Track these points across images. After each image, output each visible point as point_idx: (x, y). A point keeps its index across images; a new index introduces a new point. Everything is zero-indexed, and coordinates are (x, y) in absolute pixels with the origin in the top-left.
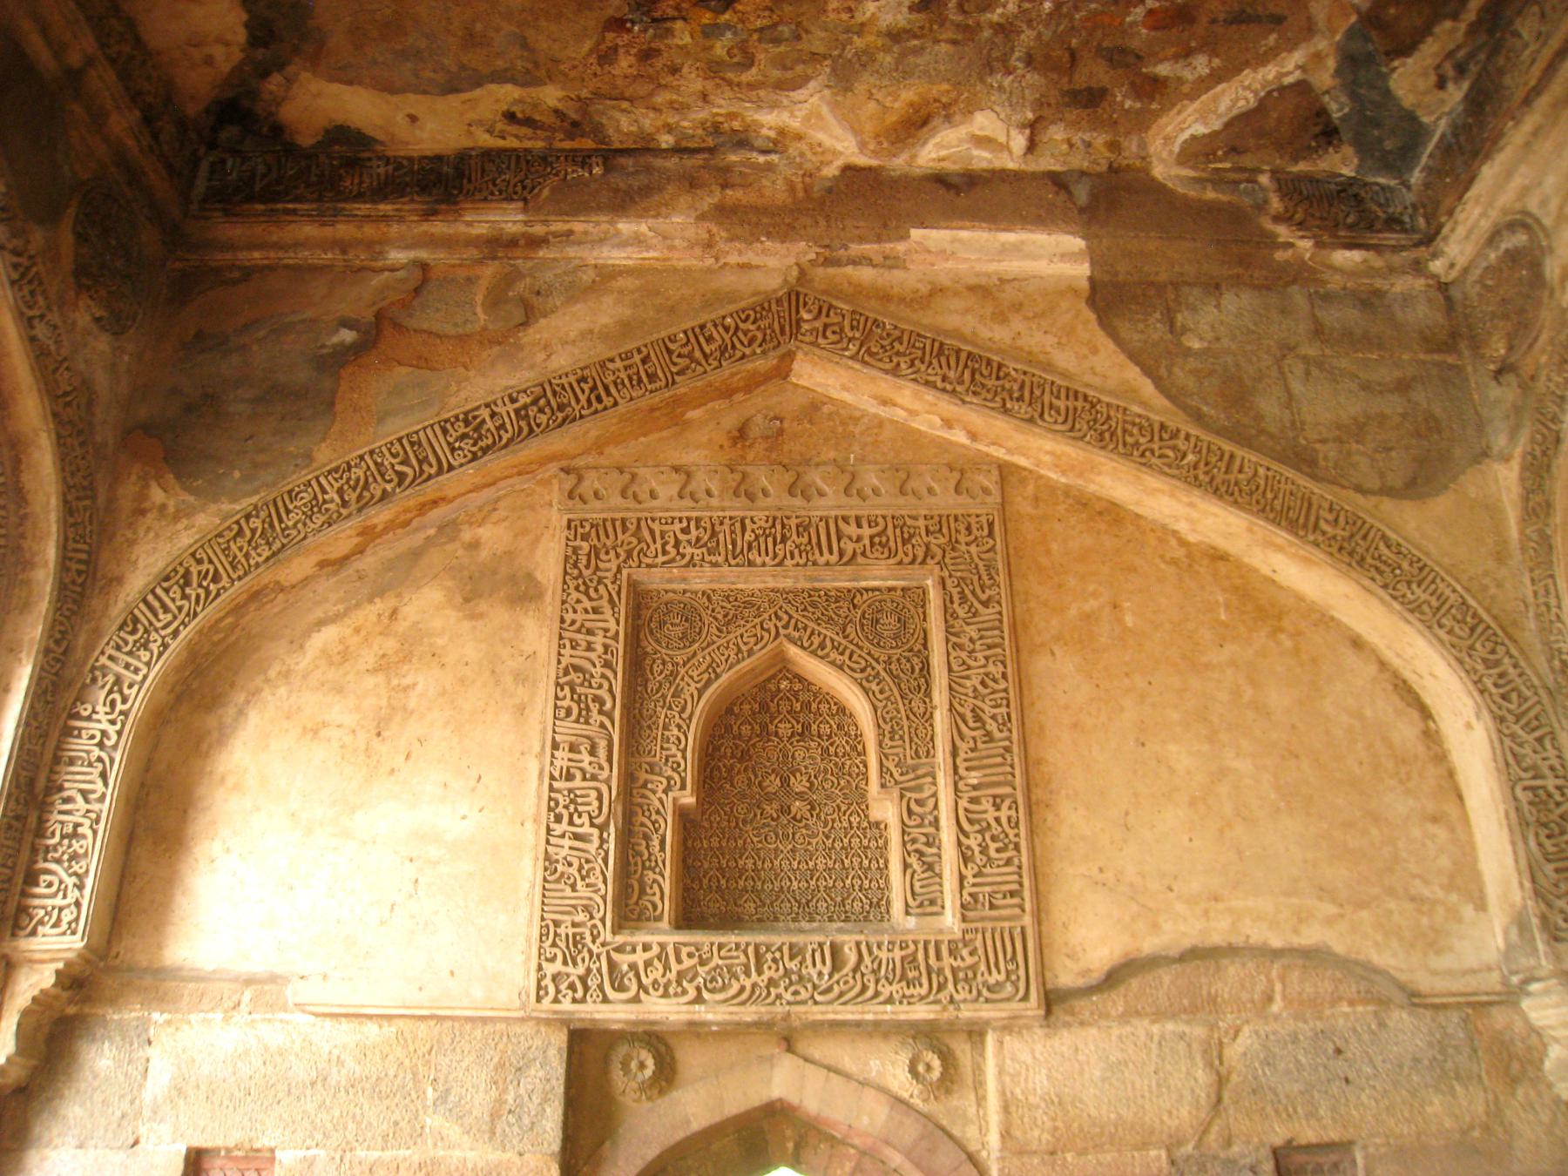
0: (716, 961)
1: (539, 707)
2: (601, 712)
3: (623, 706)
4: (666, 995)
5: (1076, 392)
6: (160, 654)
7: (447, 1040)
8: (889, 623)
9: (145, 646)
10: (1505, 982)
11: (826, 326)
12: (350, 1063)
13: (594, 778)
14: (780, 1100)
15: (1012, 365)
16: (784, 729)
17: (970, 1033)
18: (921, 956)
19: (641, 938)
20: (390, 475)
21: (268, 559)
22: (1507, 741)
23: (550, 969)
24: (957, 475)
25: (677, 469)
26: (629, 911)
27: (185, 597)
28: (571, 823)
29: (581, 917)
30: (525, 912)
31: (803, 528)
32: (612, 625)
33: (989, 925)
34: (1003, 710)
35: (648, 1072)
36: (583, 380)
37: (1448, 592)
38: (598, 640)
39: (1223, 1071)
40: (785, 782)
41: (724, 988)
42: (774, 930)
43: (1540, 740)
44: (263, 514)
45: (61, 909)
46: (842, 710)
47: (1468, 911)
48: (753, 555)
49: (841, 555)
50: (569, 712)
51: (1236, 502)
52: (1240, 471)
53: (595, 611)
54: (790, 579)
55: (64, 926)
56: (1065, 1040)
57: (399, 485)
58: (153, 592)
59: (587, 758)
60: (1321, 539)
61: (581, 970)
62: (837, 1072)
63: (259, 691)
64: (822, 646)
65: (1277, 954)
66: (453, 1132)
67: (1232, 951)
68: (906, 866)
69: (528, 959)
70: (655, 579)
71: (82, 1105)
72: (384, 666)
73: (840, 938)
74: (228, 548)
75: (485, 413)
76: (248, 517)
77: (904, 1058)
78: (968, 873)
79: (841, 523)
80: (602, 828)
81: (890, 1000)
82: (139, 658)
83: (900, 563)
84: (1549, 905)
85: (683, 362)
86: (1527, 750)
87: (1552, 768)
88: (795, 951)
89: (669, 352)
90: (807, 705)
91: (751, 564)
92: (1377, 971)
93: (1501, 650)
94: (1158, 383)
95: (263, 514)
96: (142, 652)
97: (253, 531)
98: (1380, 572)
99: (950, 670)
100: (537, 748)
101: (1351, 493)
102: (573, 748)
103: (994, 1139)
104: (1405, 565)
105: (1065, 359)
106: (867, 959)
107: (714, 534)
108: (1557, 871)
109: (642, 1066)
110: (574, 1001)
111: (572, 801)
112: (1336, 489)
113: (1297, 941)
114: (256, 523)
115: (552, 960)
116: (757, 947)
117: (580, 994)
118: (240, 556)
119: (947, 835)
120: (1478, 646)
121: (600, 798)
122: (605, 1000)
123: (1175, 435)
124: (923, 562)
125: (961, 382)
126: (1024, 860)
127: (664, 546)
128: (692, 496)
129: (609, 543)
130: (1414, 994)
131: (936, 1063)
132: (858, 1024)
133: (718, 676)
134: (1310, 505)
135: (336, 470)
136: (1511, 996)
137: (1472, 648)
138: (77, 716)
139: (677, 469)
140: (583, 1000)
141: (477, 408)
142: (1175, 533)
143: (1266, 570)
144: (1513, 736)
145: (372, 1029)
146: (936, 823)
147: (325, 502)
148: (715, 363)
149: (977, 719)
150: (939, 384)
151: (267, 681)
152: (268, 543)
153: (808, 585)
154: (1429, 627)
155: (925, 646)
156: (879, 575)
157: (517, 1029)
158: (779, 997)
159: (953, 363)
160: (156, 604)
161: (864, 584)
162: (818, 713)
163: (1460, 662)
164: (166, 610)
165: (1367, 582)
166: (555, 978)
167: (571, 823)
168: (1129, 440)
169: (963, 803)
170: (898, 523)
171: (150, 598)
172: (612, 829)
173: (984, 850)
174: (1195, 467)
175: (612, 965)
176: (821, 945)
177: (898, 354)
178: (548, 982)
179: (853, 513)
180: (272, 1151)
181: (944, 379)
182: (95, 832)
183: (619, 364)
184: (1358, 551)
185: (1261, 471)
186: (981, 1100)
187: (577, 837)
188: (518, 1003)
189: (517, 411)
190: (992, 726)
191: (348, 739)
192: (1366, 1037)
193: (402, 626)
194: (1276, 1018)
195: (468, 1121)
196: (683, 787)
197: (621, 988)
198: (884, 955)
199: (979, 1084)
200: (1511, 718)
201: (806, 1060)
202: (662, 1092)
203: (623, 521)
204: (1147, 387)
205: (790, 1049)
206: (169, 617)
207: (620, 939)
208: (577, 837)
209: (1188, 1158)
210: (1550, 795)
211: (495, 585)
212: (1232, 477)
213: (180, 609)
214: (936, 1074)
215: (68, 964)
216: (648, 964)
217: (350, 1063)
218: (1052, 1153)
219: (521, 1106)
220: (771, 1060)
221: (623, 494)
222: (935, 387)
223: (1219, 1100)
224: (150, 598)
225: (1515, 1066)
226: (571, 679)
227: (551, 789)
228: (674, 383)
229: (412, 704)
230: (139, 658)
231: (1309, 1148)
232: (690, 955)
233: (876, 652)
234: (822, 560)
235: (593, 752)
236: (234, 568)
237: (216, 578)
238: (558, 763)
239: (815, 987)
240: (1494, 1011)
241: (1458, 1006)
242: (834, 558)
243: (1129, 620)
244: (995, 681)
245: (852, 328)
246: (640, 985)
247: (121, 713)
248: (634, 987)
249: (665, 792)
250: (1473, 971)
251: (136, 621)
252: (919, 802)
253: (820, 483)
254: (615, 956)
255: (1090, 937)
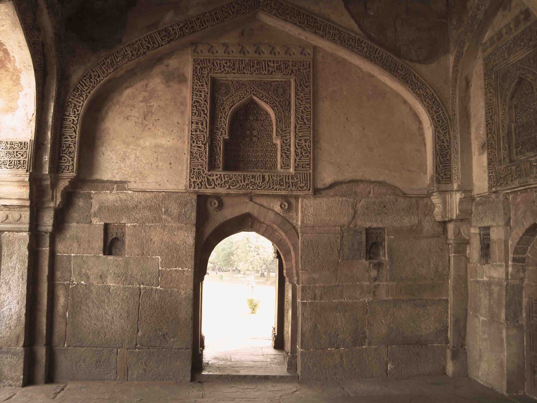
0: (234, 179)
1: (187, 112)
2: (204, 114)
3: (210, 113)
4: (221, 187)
5: (336, 28)
6: (86, 98)
7: (167, 197)
8: (281, 91)
9: (81, 96)
10: (428, 192)
11: (267, 4)
12: (143, 203)
13: (203, 131)
14: (249, 213)
15: (318, 18)
16: (251, 118)
17: (295, 198)
18: (284, 179)
19: (215, 173)
20: (145, 47)
21: (113, 71)
22: (437, 133)
23: (192, 180)
24: (301, 49)
25: (224, 44)
26: (212, 166)
27: (91, 82)
28: (197, 143)
29: (200, 167)
30: (185, 166)
31: (258, 63)
32: (206, 90)
33: (302, 172)
34: (309, 116)
35: (216, 205)
36: (198, 19)
37: (429, 92)
38: (203, 94)
39: (356, 210)
40: (251, 132)
41: (236, 185)
42: (247, 171)
43: (445, 133)
44: (110, 58)
45: (69, 166)
46: (267, 113)
47: (422, 174)
48: (245, 71)
49: (269, 71)
50: (195, 113)
51: (376, 63)
52: (378, 54)
53: (202, 85)
54: (255, 77)
55: (70, 170)
56: (318, 201)
57: (148, 49)
58: (81, 80)
59: (201, 126)
60: (397, 74)
61: (200, 181)
62: (262, 206)
63: (111, 106)
64: (263, 97)
65: (373, 182)
66: (169, 219)
67: (362, 181)
68: (282, 156)
69: (187, 177)
70: (218, 76)
71: (77, 213)
72: (145, 100)
73: (264, 174)
74: (101, 68)
75: (171, 29)
76: (106, 59)
77: (279, 203)
78: (297, 159)
79: (269, 63)
80: (205, 145)
81: (276, 190)
82: (80, 99)
83: (284, 74)
84: (439, 175)
85: (226, 14)
86: (441, 136)
87: (447, 141)
88: (253, 177)
89: (223, 11)
90: (257, 112)
91: (244, 73)
92: (396, 187)
93: (440, 109)
94: (359, 26)
95: (110, 58)
96: (81, 98)
97: (108, 63)
98: (412, 86)
99: (296, 105)
100: (187, 123)
101: (407, 62)
102: (197, 123)
103: (299, 223)
104: (419, 84)
105: (333, 18)
106: (271, 179)
107: (234, 64)
108: (443, 167)
109: (215, 204)
110: (199, 188)
111: (197, 138)
112: (404, 60)
113: (377, 180)
114: (108, 60)
115: (193, 178)
116: (244, 175)
117: (200, 186)
118: (105, 70)
119: (292, 149)
120: (434, 107)
121: (204, 137)
122: (206, 188)
123: (362, 42)
124: (291, 74)
125: (304, 23)
126: (311, 156)
127: (220, 67)
128: (228, 53)
129: (205, 66)
130: (405, 194)
131: (287, 205)
132: (268, 195)
133: (235, 104)
134: (396, 64)
135: (129, 45)
136: (429, 195)
137: (432, 107)
138: (66, 115)
139: (224, 44)
140: (201, 188)
141: (168, 27)
142: (360, 68)
143: (383, 81)
144: (439, 132)
145: (148, 195)
146: (290, 145)
147: (127, 54)
148: (235, 15)
149: (302, 118)
150: (298, 24)
151: (114, 104)
152: (112, 67)
153: (259, 80)
154: (422, 101)
155: (290, 97)
156: (278, 77)
157: (184, 194)
158: (249, 188)
159: (302, 17)
160: (83, 84)
161: (274, 80)
162: (261, 114)
163: (429, 111)
164: (86, 86)
165: (408, 88)
166: (194, 182)
167: (197, 143)
168: (349, 43)
169: (297, 141)
170: (285, 63)
171: (81, 82)
172: (207, 145)
173: (302, 153)
174: (366, 52)
175: (208, 179)
176: (260, 175)
177: (287, 14)
178: (192, 183)
179: (272, 59)
180: (125, 224)
181: (300, 22)
182: (75, 147)
183: (208, 15)
184: (407, 79)
185: (384, 54)
186: (297, 214)
187: (199, 147)
188: (184, 188)
189: (180, 28)
190: (306, 121)
191: (136, 120)
192: (392, 203)
193: (149, 89)
194: (371, 198)
195: (173, 217)
196: (225, 134)
197: (210, 185)
198: (275, 178)
199: (297, 210)
200: (439, 127)
201: (255, 203)
202: (220, 210)
203: (209, 60)
204: (356, 27)
205: (251, 200)
206: (87, 88)
207: (210, 173)
208: (199, 147)
209: (345, 229)
210: (445, 147)
211: (174, 78)
212: (376, 56)
213: (90, 85)
214: (286, 207)
215: (71, 179)
216: (217, 179)
217: (143, 203)
218: (313, 227)
219: (186, 213)
220: (247, 203)
221: (209, 52)
222: (296, 24)
223: (354, 217)
224: (81, 82)
225: (427, 212)
226: (196, 104)
227: (192, 134)
228: (224, 21)
229: (153, 111)
230: (80, 99)
231: (375, 228)
232: (227, 177)
233: (277, 99)
234: (263, 73)
235: (202, 125)
236: (104, 74)
237: (99, 77)
238: (193, 128)
239: (258, 186)
240: (425, 199)
241: (415, 197)
242: (266, 73)
243: (345, 93)
244: (307, 109)
245: (274, 5)
246: (215, 184)
247: (78, 114)
248: (214, 185)
249: (221, 135)
250: (420, 189)
251: (78, 88)
252: (286, 140)
253: (263, 50)
254: (209, 177)
255: (327, 176)
